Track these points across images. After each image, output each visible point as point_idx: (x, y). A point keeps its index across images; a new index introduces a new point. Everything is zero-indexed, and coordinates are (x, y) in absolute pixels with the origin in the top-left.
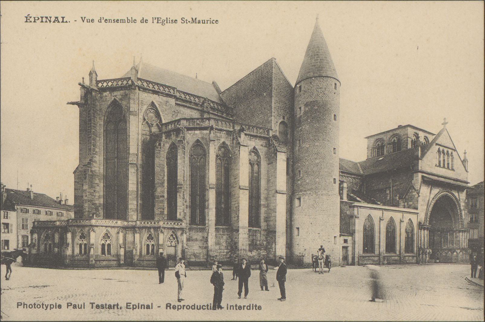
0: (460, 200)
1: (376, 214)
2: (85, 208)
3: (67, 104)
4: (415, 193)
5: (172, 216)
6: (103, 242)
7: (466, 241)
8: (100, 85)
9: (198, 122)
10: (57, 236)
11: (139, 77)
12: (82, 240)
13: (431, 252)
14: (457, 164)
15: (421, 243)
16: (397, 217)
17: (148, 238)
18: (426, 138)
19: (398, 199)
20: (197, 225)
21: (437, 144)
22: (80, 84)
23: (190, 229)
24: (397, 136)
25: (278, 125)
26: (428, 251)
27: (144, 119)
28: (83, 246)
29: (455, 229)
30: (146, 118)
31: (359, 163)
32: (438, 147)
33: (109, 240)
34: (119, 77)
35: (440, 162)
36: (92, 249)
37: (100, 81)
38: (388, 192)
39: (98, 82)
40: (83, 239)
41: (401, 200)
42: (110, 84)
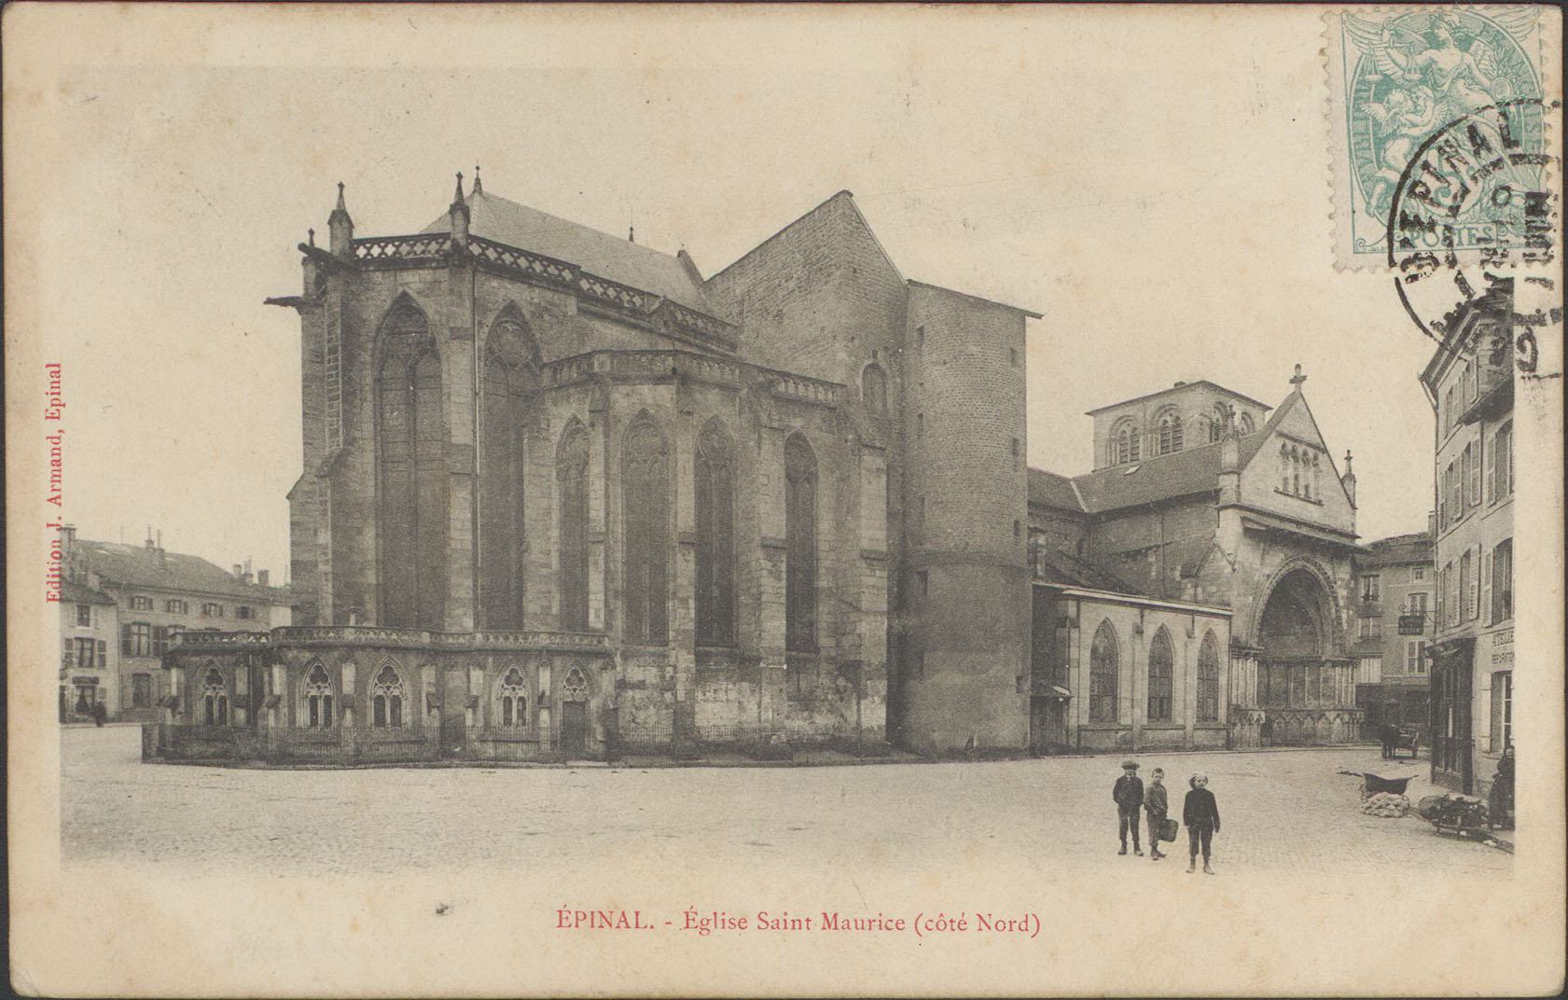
0: (1335, 583)
1: (1123, 619)
2: (324, 595)
3: (266, 303)
4: (1224, 563)
5: (574, 617)
6: (380, 692)
8: (361, 252)
9: (643, 359)
11: (472, 232)
12: (319, 687)
13: (1264, 717)
14: (1327, 487)
17: (508, 680)
21: (1281, 435)
22: (302, 247)
24: (1172, 412)
25: (861, 372)
27: (490, 350)
28: (321, 704)
29: (1323, 659)
31: (1075, 480)
34: (415, 232)
35: (1286, 479)
36: (348, 714)
37: (362, 242)
38: (1152, 559)
41: (1186, 581)
42: (390, 250)
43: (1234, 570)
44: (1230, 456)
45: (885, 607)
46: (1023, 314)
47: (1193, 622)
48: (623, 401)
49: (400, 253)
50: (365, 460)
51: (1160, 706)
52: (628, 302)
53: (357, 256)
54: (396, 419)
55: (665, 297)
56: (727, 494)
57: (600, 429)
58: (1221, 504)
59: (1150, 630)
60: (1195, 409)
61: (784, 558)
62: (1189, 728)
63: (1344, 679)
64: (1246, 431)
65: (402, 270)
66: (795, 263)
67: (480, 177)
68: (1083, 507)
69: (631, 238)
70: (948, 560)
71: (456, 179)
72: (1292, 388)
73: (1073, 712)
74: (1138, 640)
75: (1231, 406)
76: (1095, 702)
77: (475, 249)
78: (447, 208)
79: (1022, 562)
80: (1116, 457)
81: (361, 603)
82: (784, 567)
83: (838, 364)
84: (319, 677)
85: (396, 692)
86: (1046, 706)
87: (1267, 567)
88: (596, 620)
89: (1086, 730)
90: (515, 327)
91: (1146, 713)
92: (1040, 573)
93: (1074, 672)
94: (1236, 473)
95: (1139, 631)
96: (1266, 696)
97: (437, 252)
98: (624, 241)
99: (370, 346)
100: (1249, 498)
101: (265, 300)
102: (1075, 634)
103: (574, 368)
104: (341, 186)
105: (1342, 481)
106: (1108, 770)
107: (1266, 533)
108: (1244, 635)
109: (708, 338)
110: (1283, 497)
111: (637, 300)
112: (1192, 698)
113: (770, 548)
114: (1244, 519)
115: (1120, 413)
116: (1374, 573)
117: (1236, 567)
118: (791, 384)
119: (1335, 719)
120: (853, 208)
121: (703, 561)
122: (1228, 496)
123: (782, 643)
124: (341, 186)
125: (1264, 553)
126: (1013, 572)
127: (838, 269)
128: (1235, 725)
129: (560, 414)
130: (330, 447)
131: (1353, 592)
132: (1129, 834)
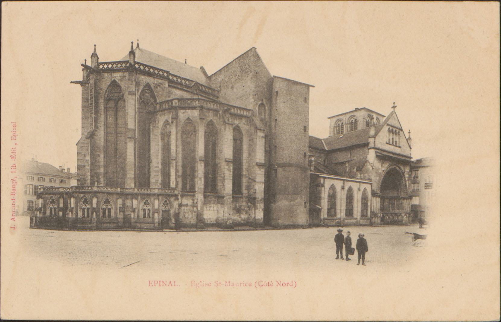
1: (338, 184)
3: (70, 83)
4: (370, 166)
5: (166, 184)
6: (104, 207)
7: (409, 207)
8: (101, 67)
9: (189, 102)
10: (61, 201)
11: (136, 60)
12: (85, 205)
14: (403, 142)
15: (374, 208)
16: (355, 186)
17: (145, 203)
18: (377, 119)
19: (355, 171)
20: (188, 192)
21: (388, 125)
22: (82, 65)
23: (182, 196)
26: (379, 215)
27: (141, 98)
28: (86, 210)
29: (401, 197)
30: (143, 97)
31: (324, 139)
32: (388, 127)
33: (110, 205)
34: (118, 60)
36: (94, 214)
37: (102, 63)
38: (347, 165)
39: (100, 64)
40: (85, 204)
41: (358, 172)
42: (110, 66)
43: (373, 169)
44: (372, 132)
45: (263, 180)
46: (308, 86)
47: (360, 185)
48: (183, 115)
49: (113, 67)
50: (101, 133)
51: (349, 212)
52: (184, 83)
53: (100, 68)
54: (111, 120)
55: (196, 81)
56: (214, 145)
57: (175, 124)
58: (369, 148)
59: (346, 188)
60: (361, 116)
61: (232, 165)
62: (359, 219)
63: (407, 203)
64: (377, 124)
65: (114, 73)
66: (237, 70)
67: (139, 43)
68: (326, 148)
69: (186, 63)
70: (284, 165)
71: (131, 44)
72: (392, 110)
73: (322, 214)
74: (343, 191)
75: (373, 116)
76: (329, 210)
77: (137, 66)
78: (128, 53)
79: (307, 166)
80: (336, 132)
81: (98, 178)
82: (232, 168)
83: (251, 103)
84: (86, 202)
85: (110, 207)
86: (314, 212)
87: (382, 168)
88: (173, 185)
89: (326, 219)
90: (148, 91)
91: (345, 214)
92: (312, 170)
93: (322, 201)
94: (373, 137)
95: (343, 188)
96: (382, 209)
97: (125, 67)
98: (183, 63)
99: (103, 96)
100: (378, 145)
101: (70, 82)
102: (323, 189)
103: (167, 105)
104: (95, 45)
105: (407, 140)
106: (334, 231)
107: (383, 157)
108: (376, 190)
109: (208, 94)
110: (388, 145)
111: (187, 83)
112: (359, 210)
113: (227, 161)
114: (376, 152)
115: (338, 118)
116: (417, 169)
117: (374, 167)
118: (236, 110)
119: (404, 216)
120: (256, 52)
121: (206, 166)
122: (371, 145)
123: (231, 192)
124: (95, 45)
125: (383, 163)
126: (304, 169)
127: (251, 72)
128: (373, 218)
129: (162, 119)
130: (90, 129)
131: (410, 176)
132: (339, 253)
